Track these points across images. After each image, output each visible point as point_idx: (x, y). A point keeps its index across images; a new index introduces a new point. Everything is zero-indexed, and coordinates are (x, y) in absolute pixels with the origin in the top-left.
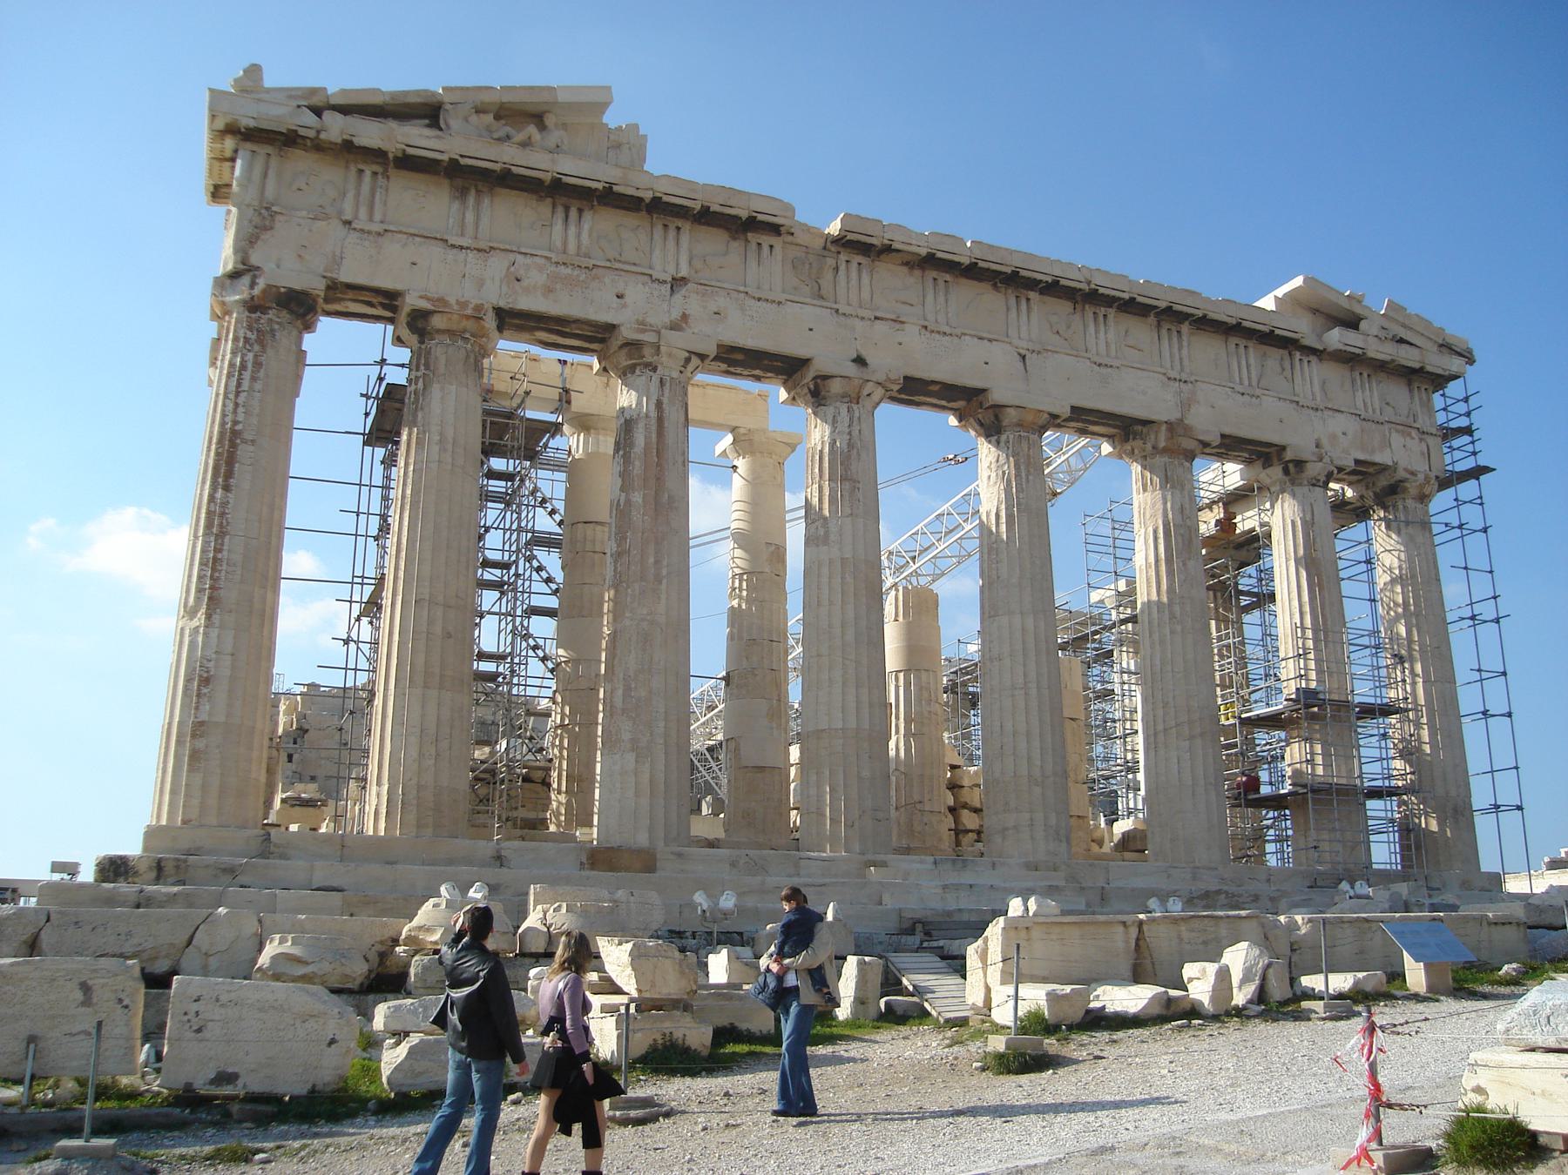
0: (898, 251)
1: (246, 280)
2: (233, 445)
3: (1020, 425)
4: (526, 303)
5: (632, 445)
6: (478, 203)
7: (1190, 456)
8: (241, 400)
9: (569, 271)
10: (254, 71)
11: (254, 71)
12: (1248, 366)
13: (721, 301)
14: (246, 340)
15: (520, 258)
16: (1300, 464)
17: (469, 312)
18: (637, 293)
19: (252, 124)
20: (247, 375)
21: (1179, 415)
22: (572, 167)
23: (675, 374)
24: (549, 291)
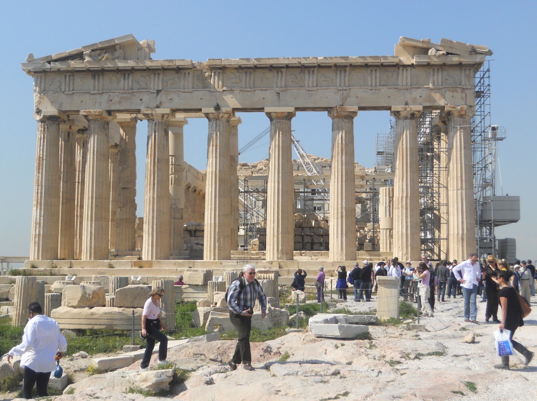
0: (228, 68)
3: (278, 118)
6: (99, 78)
7: (351, 116)
10: (31, 56)
11: (31, 56)
12: (376, 78)
13: (172, 95)
15: (111, 94)
16: (398, 112)
17: (97, 114)
18: (146, 98)
21: (341, 103)
22: (121, 64)
23: (160, 121)
24: (120, 102)
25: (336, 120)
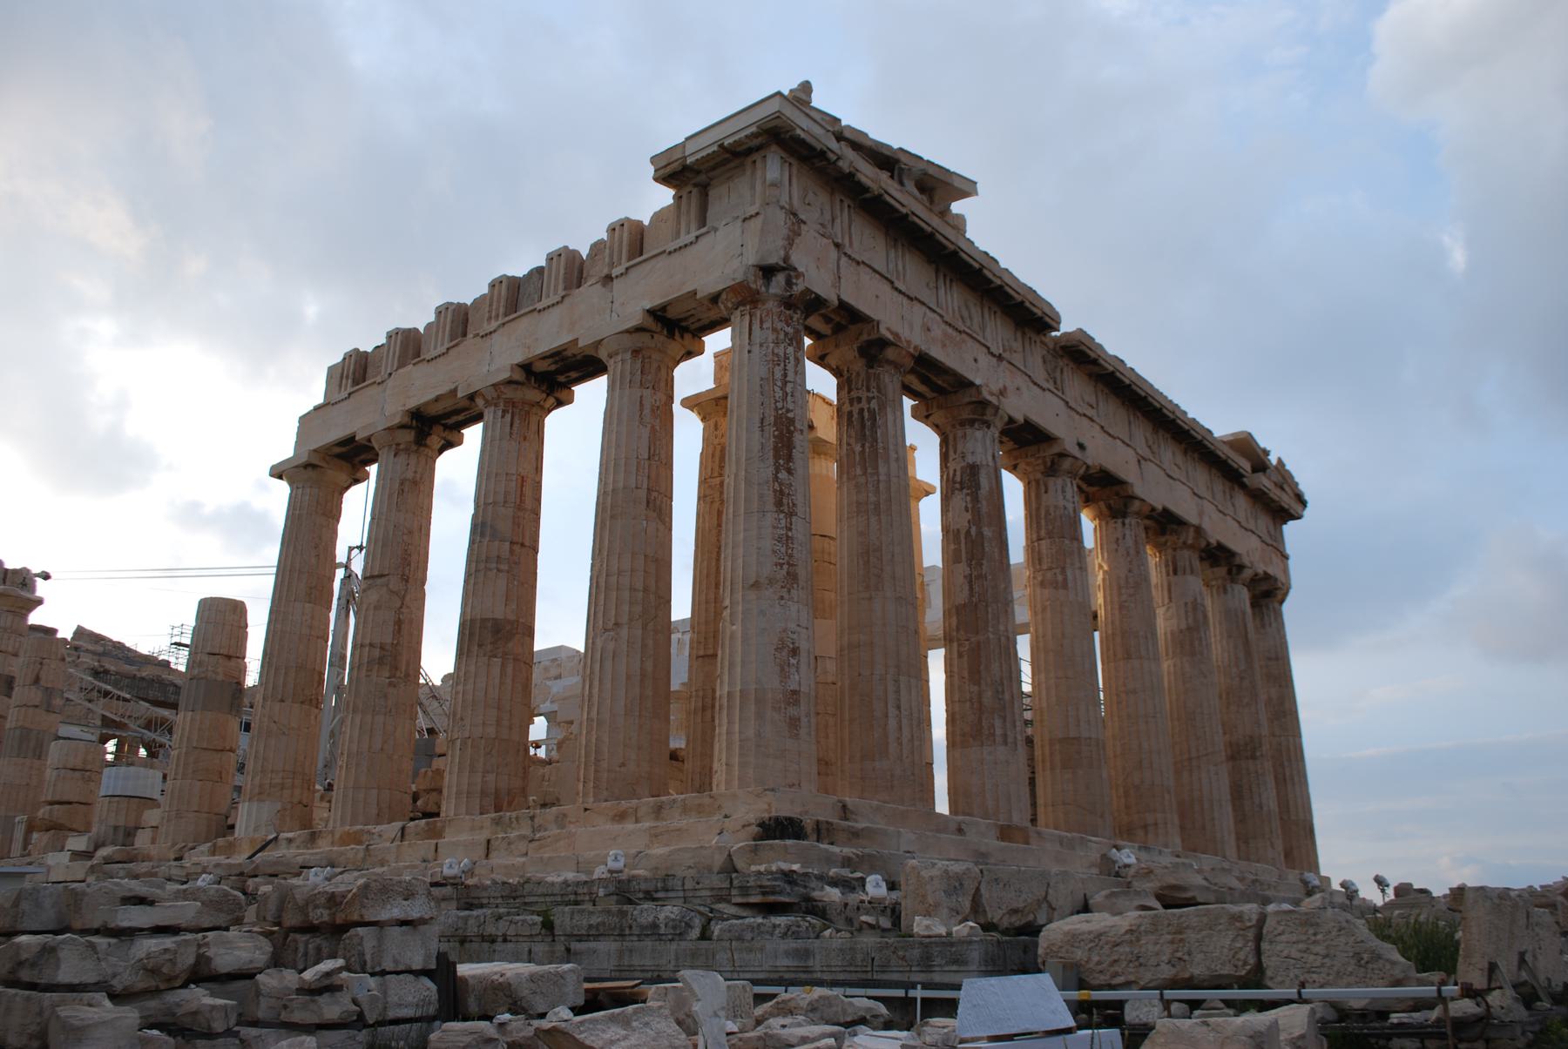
1: (780, 278)
2: (791, 433)
3: (1138, 514)
4: (936, 353)
5: (978, 487)
8: (789, 389)
9: (950, 331)
10: (806, 87)
11: (806, 87)
13: (1020, 380)
14: (786, 334)
16: (1241, 567)
18: (985, 360)
19: (803, 135)
20: (790, 367)
24: (944, 346)
25: (1186, 553)
